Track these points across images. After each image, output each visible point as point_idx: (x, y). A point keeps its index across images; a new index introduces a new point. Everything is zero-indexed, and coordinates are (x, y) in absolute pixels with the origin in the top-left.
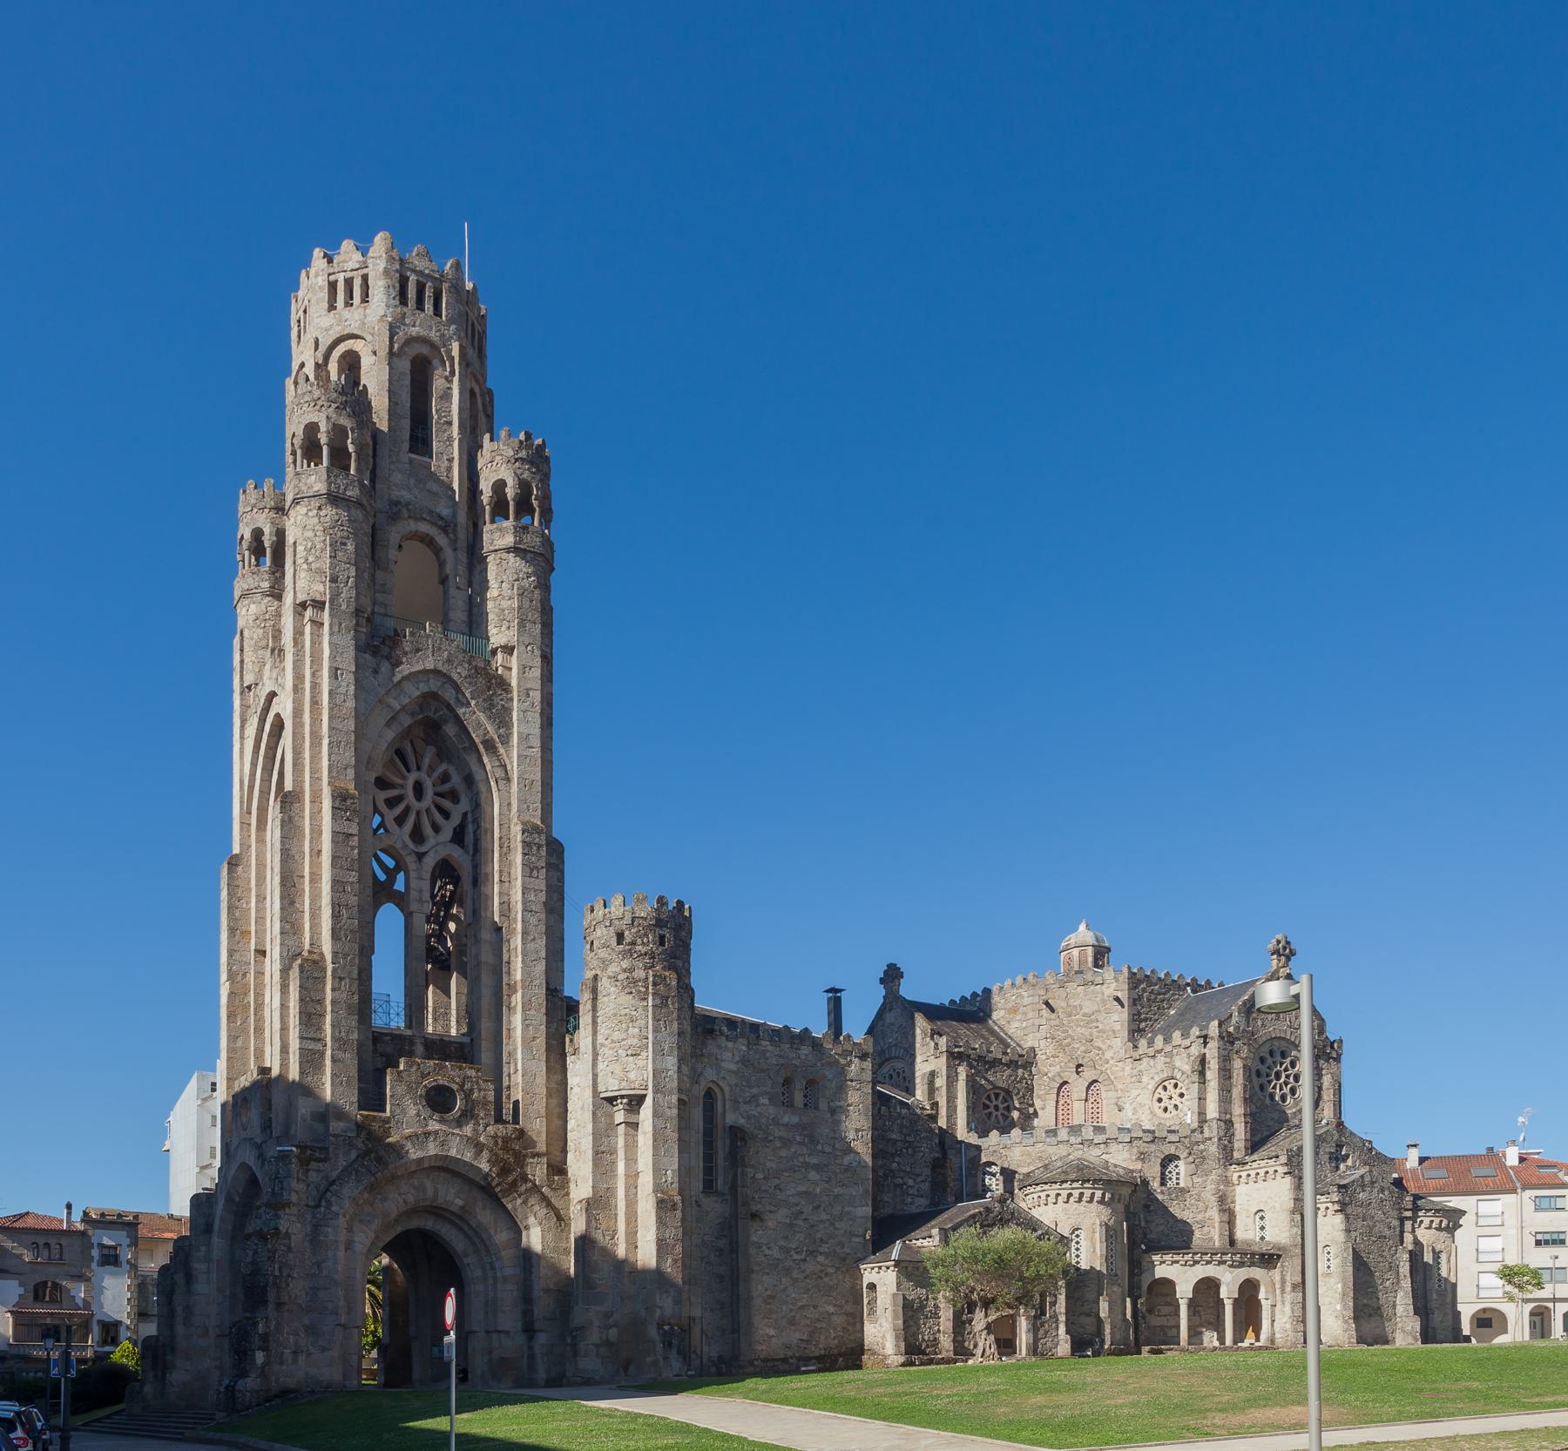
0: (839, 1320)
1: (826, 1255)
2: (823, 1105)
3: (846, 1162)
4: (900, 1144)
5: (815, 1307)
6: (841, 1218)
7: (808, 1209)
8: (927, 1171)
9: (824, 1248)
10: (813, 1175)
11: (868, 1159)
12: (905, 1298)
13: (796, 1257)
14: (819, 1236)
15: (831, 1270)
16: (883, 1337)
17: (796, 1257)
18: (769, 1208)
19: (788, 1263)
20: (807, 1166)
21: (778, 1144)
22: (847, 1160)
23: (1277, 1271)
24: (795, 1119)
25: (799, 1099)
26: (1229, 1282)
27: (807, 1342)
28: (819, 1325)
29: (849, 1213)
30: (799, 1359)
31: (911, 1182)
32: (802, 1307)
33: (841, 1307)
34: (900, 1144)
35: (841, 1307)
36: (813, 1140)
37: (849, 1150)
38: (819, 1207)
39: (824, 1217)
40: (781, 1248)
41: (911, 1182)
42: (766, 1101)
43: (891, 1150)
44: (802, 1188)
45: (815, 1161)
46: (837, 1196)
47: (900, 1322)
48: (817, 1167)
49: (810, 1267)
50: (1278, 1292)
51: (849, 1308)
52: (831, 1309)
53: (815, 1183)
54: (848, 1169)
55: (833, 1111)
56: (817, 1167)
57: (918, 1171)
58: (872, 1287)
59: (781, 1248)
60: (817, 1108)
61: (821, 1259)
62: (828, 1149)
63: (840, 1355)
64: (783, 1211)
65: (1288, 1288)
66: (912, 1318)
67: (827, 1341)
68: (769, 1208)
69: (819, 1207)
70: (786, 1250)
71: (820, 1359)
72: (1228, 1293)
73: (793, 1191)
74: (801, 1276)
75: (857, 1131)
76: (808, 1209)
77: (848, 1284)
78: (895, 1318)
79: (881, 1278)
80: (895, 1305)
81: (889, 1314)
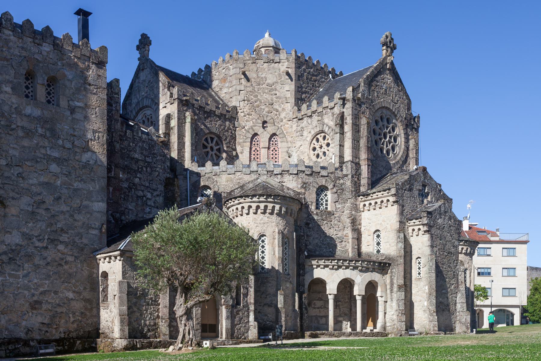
0: (78, 305)
1: (66, 244)
2: (63, 103)
3: (84, 160)
4: (141, 163)
5: (56, 293)
6: (79, 210)
7: (49, 199)
8: (161, 188)
9: (64, 237)
10: (54, 167)
11: (104, 159)
12: (128, 284)
13: (38, 244)
14: (59, 225)
15: (70, 259)
16: (113, 322)
17: (38, 244)
18: (11, 194)
19: (30, 250)
20: (50, 159)
21: (21, 133)
22: (86, 157)
23: (388, 277)
24: (37, 112)
25: (41, 92)
26: (360, 282)
27: (48, 325)
28: (59, 310)
29: (87, 207)
30: (39, 342)
31: (149, 195)
32: (43, 293)
33: (79, 293)
34: (141, 163)
35: (79, 293)
36: (54, 134)
37: (87, 149)
38: (59, 198)
39: (64, 208)
40: (24, 234)
41: (149, 195)
42: (8, 89)
43: (135, 167)
44: (42, 179)
45: (56, 154)
46: (76, 190)
47: (125, 308)
48: (58, 161)
49: (51, 254)
50: (388, 291)
51: (87, 294)
52: (71, 295)
53: (56, 176)
54: (86, 165)
55: (72, 110)
57: (154, 186)
58: (105, 275)
59: (24, 234)
60: (58, 105)
61: (61, 247)
62: (68, 145)
63: (78, 338)
64: (26, 199)
65: (395, 289)
66: (135, 304)
67: (66, 326)
68: (11, 194)
69: (59, 198)
70: (27, 237)
71: (59, 341)
72: (358, 290)
73: (35, 181)
74: (42, 263)
75: (94, 132)
76: (49, 199)
77: (86, 273)
78: (121, 304)
79: (112, 267)
80: (121, 292)
81: (117, 300)
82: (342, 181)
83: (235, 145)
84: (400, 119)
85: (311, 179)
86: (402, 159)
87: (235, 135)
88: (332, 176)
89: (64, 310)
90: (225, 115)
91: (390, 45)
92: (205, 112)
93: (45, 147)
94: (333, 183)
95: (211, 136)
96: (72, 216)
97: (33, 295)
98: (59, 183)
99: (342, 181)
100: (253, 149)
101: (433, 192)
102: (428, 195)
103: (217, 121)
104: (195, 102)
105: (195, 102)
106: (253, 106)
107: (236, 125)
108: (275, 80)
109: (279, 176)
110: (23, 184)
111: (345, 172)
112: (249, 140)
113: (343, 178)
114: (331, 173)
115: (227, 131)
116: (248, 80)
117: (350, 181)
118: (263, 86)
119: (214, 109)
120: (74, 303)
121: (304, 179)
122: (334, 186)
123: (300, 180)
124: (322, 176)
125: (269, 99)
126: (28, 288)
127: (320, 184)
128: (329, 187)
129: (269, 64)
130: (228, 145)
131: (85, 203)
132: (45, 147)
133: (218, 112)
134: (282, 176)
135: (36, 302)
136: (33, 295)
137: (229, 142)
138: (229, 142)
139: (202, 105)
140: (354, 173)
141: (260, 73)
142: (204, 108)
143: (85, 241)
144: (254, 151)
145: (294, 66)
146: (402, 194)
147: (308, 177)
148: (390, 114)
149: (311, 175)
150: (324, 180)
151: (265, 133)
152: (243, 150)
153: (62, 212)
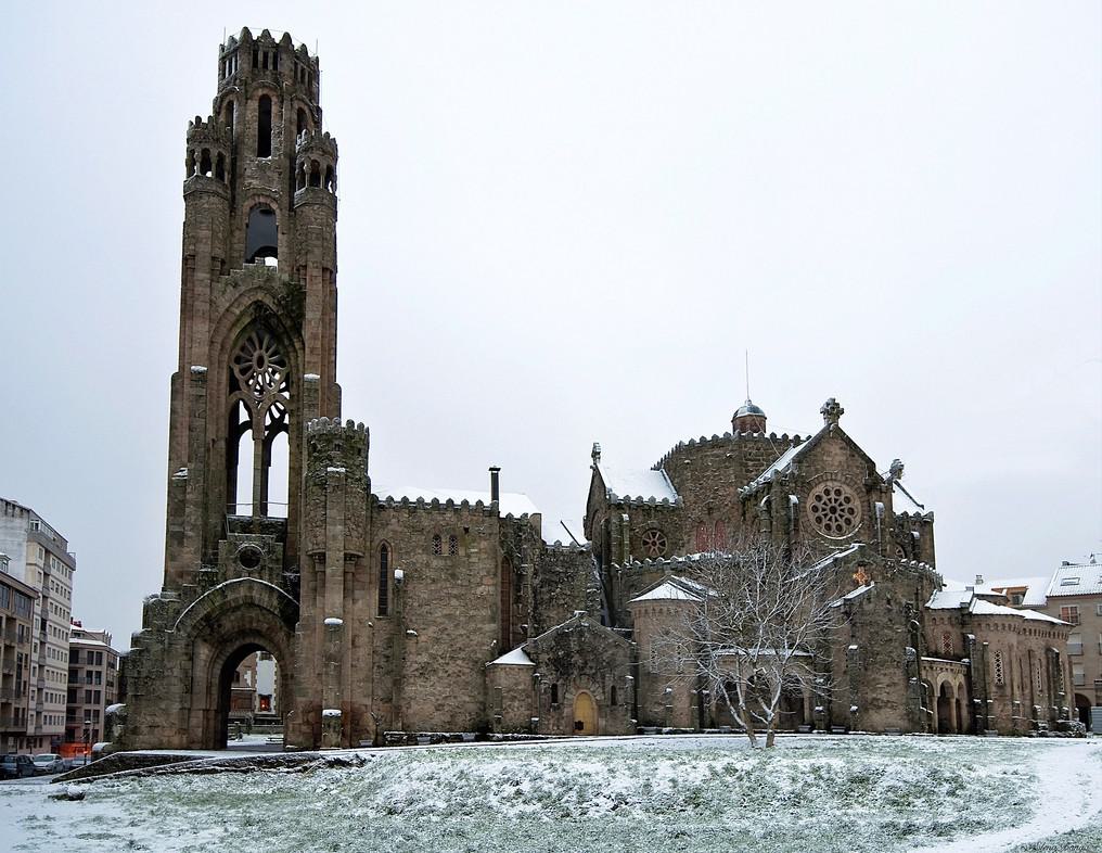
1: (463, 659)
5: (455, 697)
6: (475, 631)
7: (450, 627)
9: (462, 655)
10: (454, 602)
14: (458, 645)
17: (441, 661)
20: (450, 596)
28: (457, 710)
38: (458, 624)
40: (431, 655)
44: (445, 612)
48: (456, 596)
49: (451, 669)
52: (467, 699)
56: (456, 596)
59: (431, 655)
69: (458, 624)
70: (433, 657)
73: (440, 614)
76: (450, 627)
89: (462, 711)
91: (833, 411)
93: (447, 588)
96: (468, 637)
97: (438, 700)
98: (458, 612)
110: (430, 617)
120: (467, 706)
126: (434, 695)
131: (479, 626)
132: (447, 588)
135: (440, 705)
136: (438, 700)
143: (479, 655)
153: (461, 635)
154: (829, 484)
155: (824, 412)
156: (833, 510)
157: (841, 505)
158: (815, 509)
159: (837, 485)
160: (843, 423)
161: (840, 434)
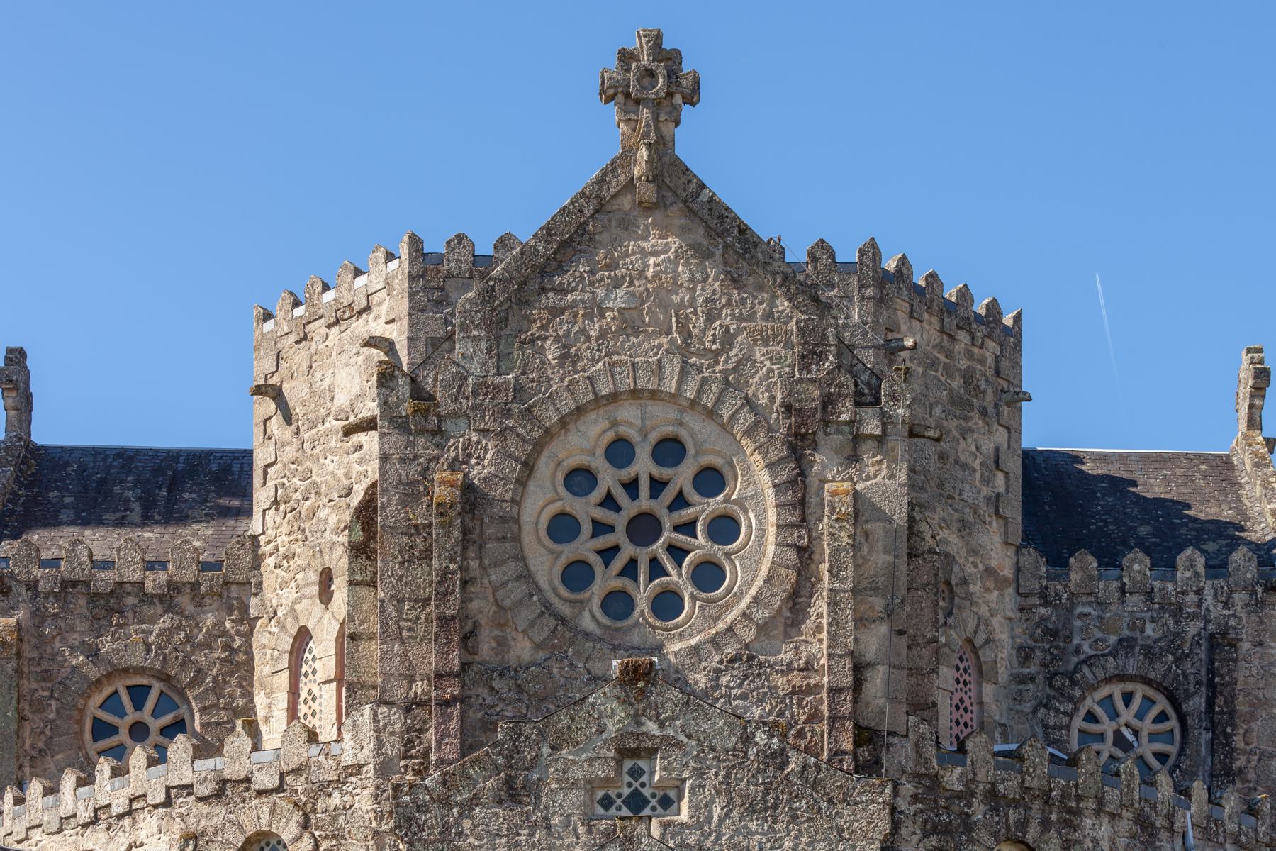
82: (336, 799)
83: (249, 695)
84: (746, 419)
85: (219, 813)
86: (761, 614)
87: (249, 652)
88: (299, 783)
90: (195, 585)
91: (655, 84)
92: (94, 598)
94: (298, 816)
95: (130, 682)
99: (336, 799)
100: (304, 694)
101: (713, 778)
102: (680, 798)
103: (153, 621)
104: (38, 573)
105: (38, 573)
106: (298, 518)
107: (253, 612)
108: (355, 390)
109: (127, 822)
111: (348, 759)
112: (284, 662)
113: (341, 782)
114: (296, 771)
115: (207, 645)
116: (288, 419)
117: (370, 790)
118: (327, 424)
119: (137, 576)
121: (191, 819)
122: (305, 826)
123: (177, 827)
124: (260, 793)
125: (340, 473)
127: (250, 830)
128: (285, 837)
129: (343, 325)
130: (212, 699)
133: (154, 582)
134: (134, 821)
137: (217, 687)
138: (217, 687)
139: (78, 576)
140: (393, 747)
141: (318, 376)
142: (87, 584)
144: (305, 702)
145: (404, 305)
146: (445, 829)
147: (204, 808)
148: (672, 414)
149: (218, 795)
150: (266, 808)
151: (328, 615)
152: (270, 703)
154: (629, 413)
155: (608, 96)
156: (644, 528)
157: (609, 502)
158: (563, 527)
159: (662, 420)
160: (699, 142)
161: (674, 190)
